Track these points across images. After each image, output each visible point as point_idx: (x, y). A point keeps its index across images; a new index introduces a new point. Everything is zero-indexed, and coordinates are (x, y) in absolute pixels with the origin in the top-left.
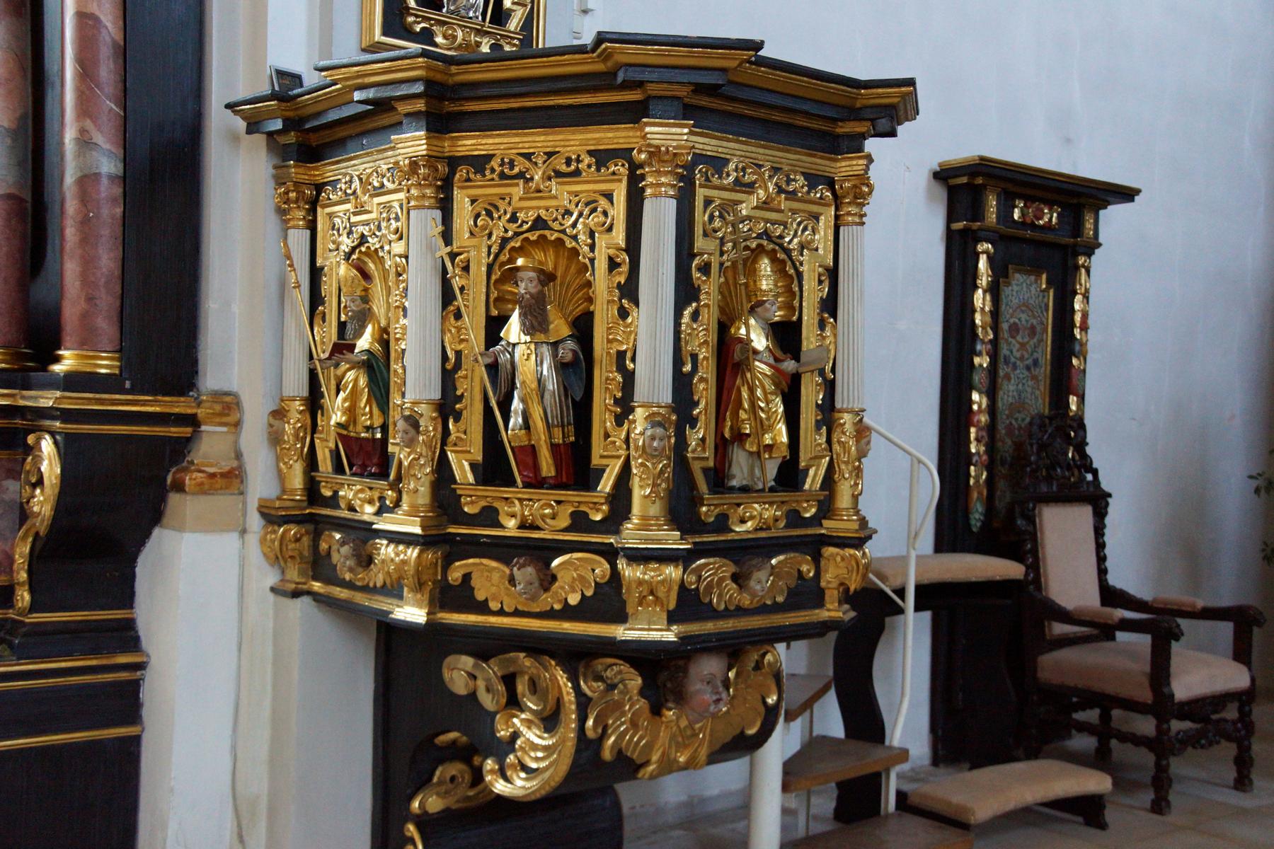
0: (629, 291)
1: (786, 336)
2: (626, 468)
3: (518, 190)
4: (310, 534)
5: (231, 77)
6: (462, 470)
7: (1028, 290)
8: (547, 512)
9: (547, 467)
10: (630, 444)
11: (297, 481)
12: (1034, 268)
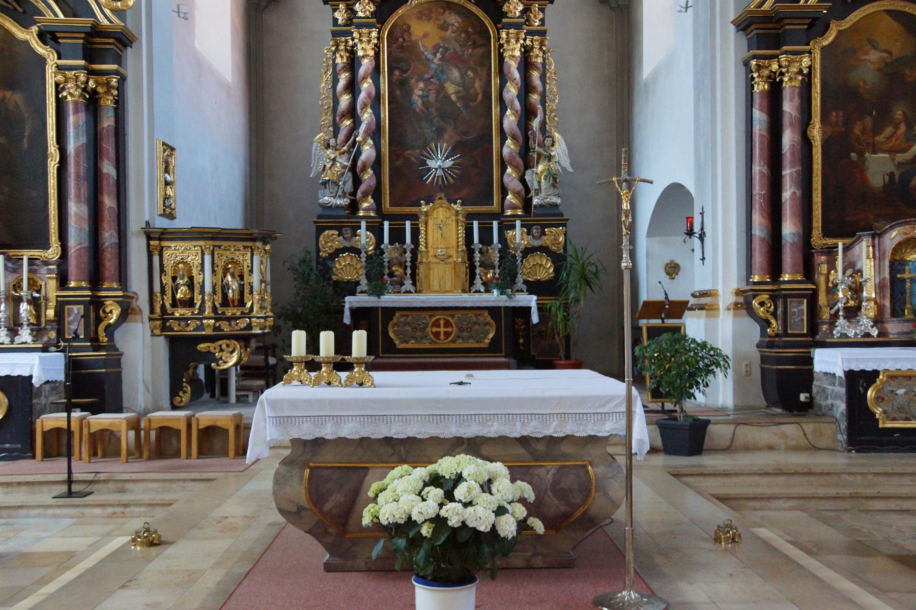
0: (251, 271)
2: (252, 303)
3: (228, 252)
4: (162, 321)
9: (236, 304)
11: (158, 310)
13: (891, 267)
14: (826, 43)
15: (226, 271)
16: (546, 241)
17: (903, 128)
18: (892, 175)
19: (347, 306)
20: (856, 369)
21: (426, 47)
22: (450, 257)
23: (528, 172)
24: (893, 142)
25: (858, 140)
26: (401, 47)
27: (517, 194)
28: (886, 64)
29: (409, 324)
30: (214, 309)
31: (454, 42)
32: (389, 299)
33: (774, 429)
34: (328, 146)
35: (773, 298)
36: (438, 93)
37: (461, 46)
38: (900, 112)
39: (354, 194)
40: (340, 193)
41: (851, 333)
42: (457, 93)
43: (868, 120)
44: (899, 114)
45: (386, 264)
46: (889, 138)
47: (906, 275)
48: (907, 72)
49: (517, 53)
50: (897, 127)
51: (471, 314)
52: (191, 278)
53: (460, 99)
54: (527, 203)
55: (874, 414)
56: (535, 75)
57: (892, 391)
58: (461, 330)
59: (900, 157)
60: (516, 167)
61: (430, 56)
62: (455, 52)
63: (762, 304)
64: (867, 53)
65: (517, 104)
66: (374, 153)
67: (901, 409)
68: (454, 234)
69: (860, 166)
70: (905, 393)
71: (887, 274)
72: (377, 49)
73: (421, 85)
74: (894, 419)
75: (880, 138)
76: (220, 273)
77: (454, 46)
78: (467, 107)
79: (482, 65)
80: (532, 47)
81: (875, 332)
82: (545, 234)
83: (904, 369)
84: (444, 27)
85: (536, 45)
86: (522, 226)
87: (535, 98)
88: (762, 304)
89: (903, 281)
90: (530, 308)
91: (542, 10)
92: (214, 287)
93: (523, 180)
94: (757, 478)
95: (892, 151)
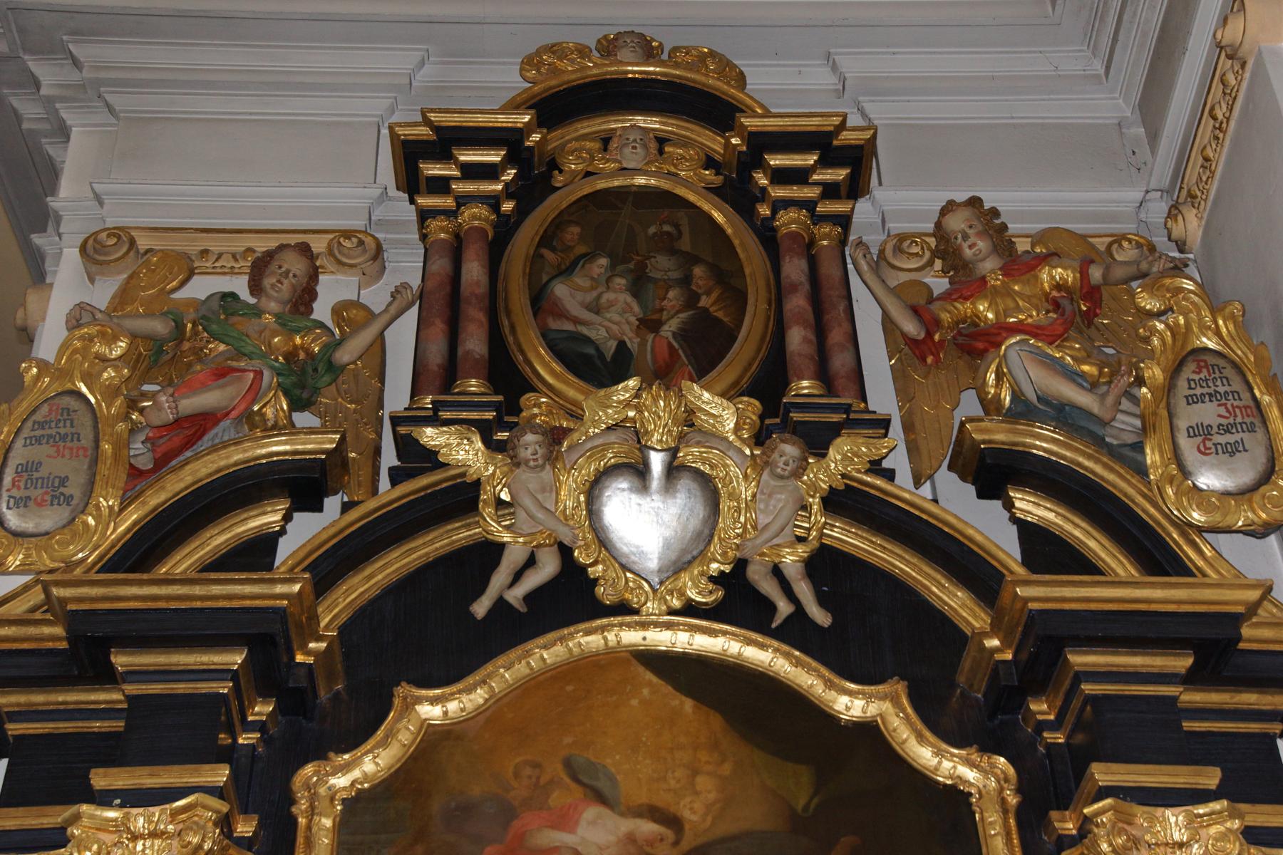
64: (565, 821)
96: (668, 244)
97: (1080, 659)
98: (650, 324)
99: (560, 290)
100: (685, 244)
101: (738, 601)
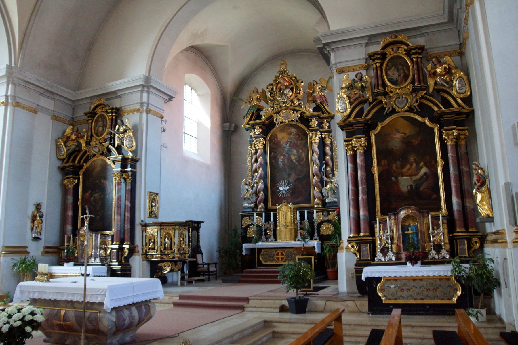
0: (175, 237)
1: (183, 239)
4: (146, 256)
5: (137, 221)
6: (162, 249)
7: (195, 232)
8: (169, 252)
10: (175, 248)
11: (144, 251)
12: (195, 230)
13: (402, 228)
14: (377, 132)
15: (165, 237)
16: (330, 217)
17: (414, 165)
18: (411, 186)
19: (244, 248)
20: (370, 276)
21: (283, 142)
22: (288, 226)
23: (323, 189)
24: (410, 172)
25: (395, 172)
26: (274, 144)
27: (319, 198)
28: (404, 138)
29: (267, 254)
30: (161, 251)
31: (294, 140)
32: (260, 244)
33: (343, 303)
34: (246, 184)
35: (357, 244)
36: (288, 160)
37: (297, 140)
38: (412, 158)
39: (256, 202)
40: (250, 202)
41: (383, 259)
42: (295, 159)
43: (398, 163)
44: (412, 159)
45: (264, 230)
46: (409, 169)
47: (410, 232)
48: (414, 141)
49: (317, 141)
50: (411, 165)
51: (291, 250)
52: (154, 240)
53: (297, 161)
54: (323, 201)
55: (380, 297)
56: (328, 149)
57: (388, 287)
58: (287, 257)
59: (414, 178)
60: (318, 187)
61: (285, 146)
62: (294, 143)
63: (352, 246)
64: (395, 135)
65: (318, 161)
66: (263, 186)
67: (393, 294)
68: (289, 216)
69: (397, 182)
70: (394, 287)
71: (400, 232)
72: (265, 146)
73: (282, 157)
74: (390, 299)
75: (404, 170)
76: (163, 238)
77: (294, 141)
78: (299, 164)
79: (305, 147)
80: (325, 138)
81: (394, 259)
82: (329, 214)
83: (420, 276)
84: (290, 134)
85: (327, 137)
86: (317, 212)
87: (328, 157)
88: (352, 246)
89: (408, 234)
90: (314, 247)
91: (329, 122)
92: (161, 243)
93: (321, 192)
94: (304, 325)
95: (411, 175)
96: (400, 64)
97: (444, 116)
98: (399, 76)
99: (389, 72)
100: (403, 64)
101: (410, 110)
